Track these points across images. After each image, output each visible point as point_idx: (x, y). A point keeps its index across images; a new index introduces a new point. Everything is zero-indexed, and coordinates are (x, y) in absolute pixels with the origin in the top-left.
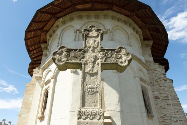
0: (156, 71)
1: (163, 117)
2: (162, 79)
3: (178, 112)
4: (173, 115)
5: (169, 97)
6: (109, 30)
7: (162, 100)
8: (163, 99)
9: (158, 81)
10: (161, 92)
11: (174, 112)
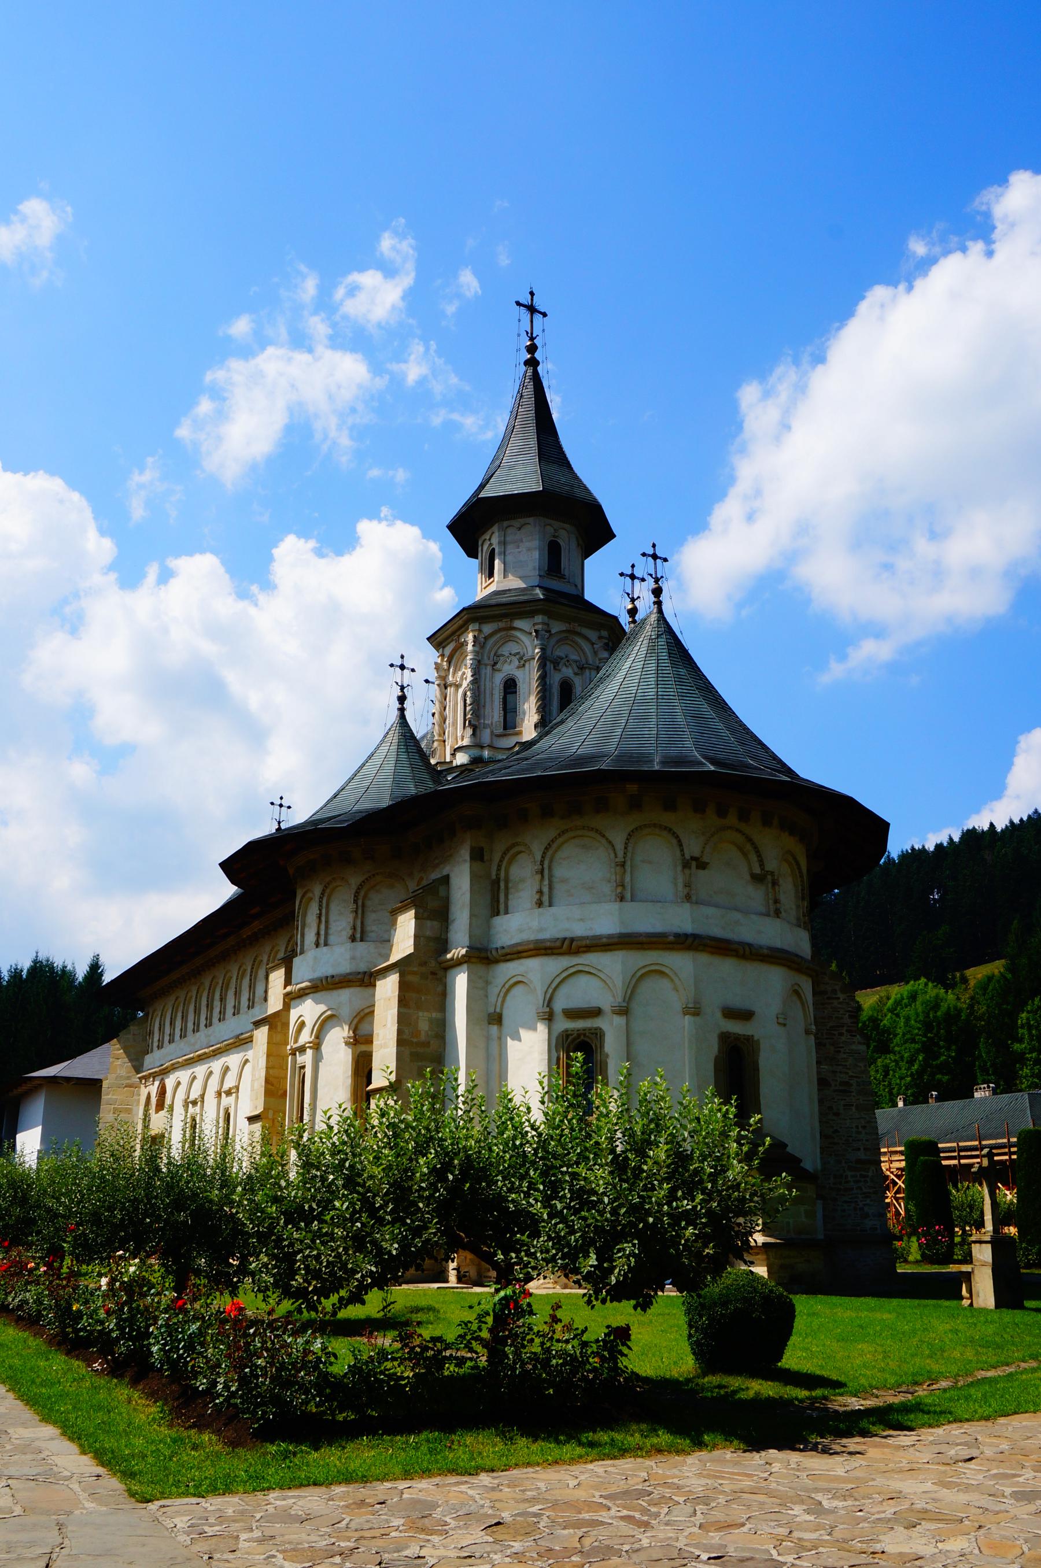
0: (835, 1002)
3: (864, 1127)
5: (852, 1085)
6: (772, 873)
7: (835, 1091)
9: (836, 1033)
11: (857, 1127)
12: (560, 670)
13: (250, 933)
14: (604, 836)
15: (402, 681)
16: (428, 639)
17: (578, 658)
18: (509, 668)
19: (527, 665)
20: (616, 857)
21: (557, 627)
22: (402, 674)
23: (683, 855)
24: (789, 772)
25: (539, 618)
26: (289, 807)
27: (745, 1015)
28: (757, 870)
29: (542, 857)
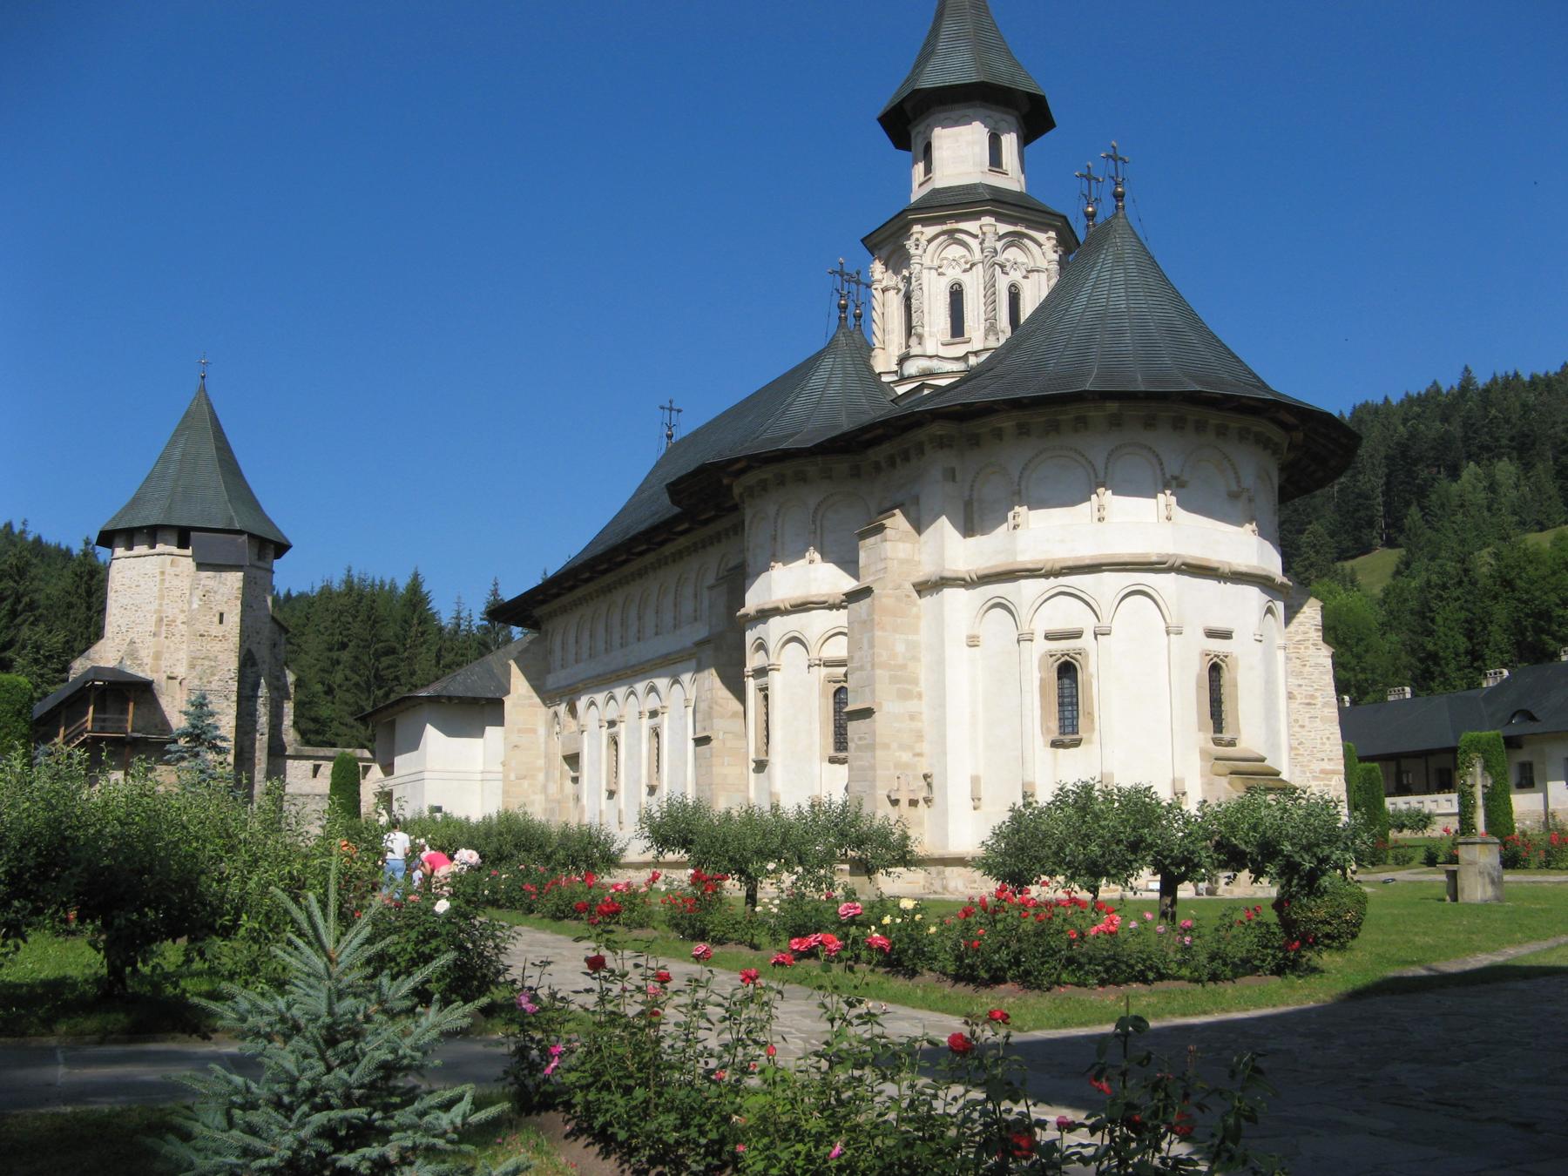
1: (1296, 749)
2: (1311, 642)
3: (1328, 738)
4: (1318, 746)
8: (1303, 701)
9: (1302, 647)
10: (1301, 682)
11: (1322, 739)
12: (1007, 274)
13: (673, 551)
14: (1083, 456)
16: (862, 241)
17: (1026, 260)
18: (954, 274)
19: (974, 268)
20: (1097, 477)
21: (1004, 228)
23: (1164, 474)
24: (1265, 387)
25: (987, 220)
26: (679, 411)
27: (1226, 635)
28: (1234, 488)
29: (1020, 477)
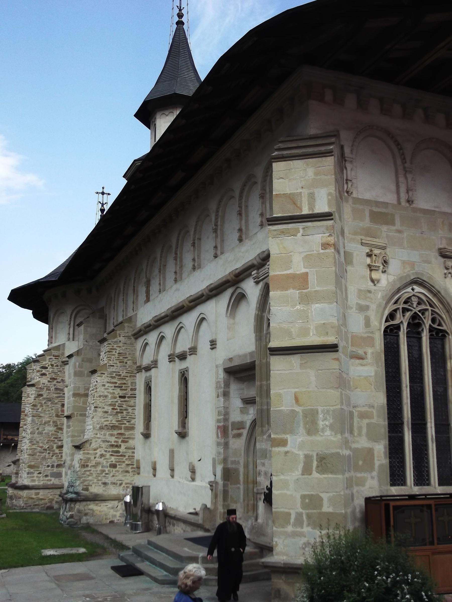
15: (103, 201)
22: (103, 197)
